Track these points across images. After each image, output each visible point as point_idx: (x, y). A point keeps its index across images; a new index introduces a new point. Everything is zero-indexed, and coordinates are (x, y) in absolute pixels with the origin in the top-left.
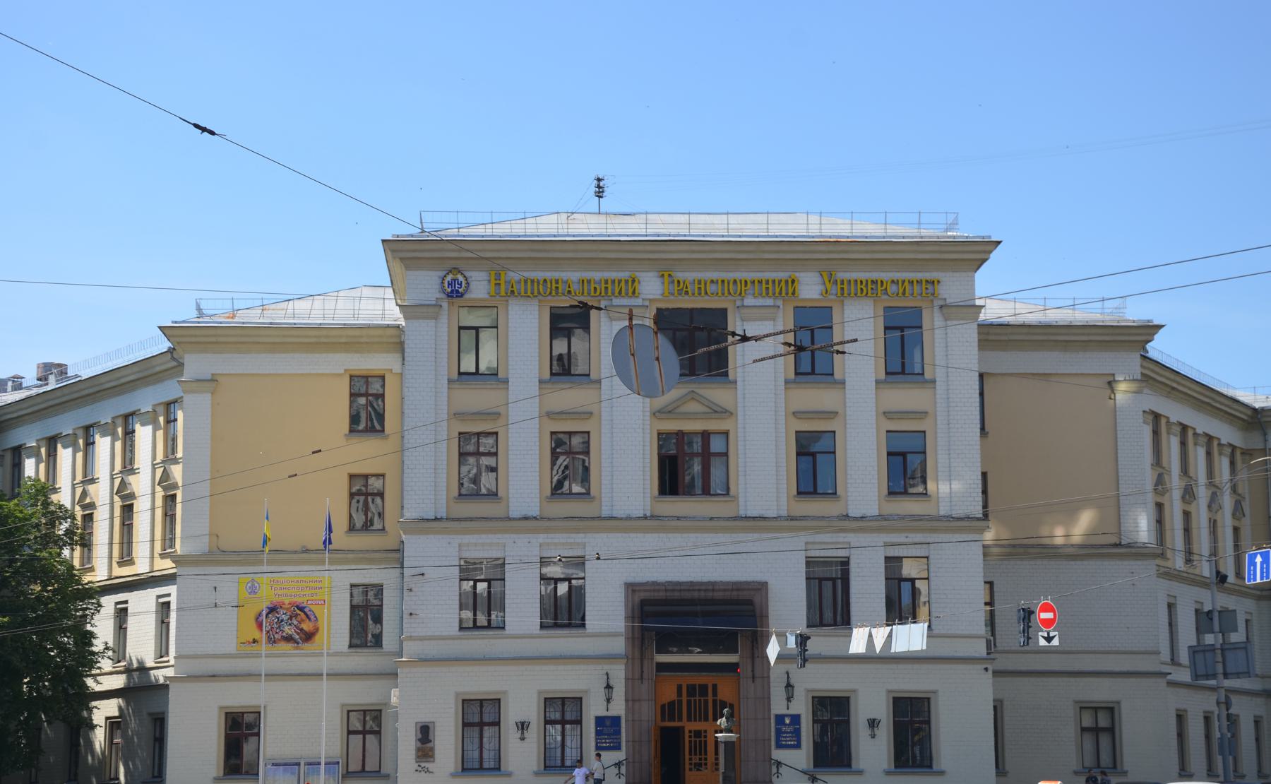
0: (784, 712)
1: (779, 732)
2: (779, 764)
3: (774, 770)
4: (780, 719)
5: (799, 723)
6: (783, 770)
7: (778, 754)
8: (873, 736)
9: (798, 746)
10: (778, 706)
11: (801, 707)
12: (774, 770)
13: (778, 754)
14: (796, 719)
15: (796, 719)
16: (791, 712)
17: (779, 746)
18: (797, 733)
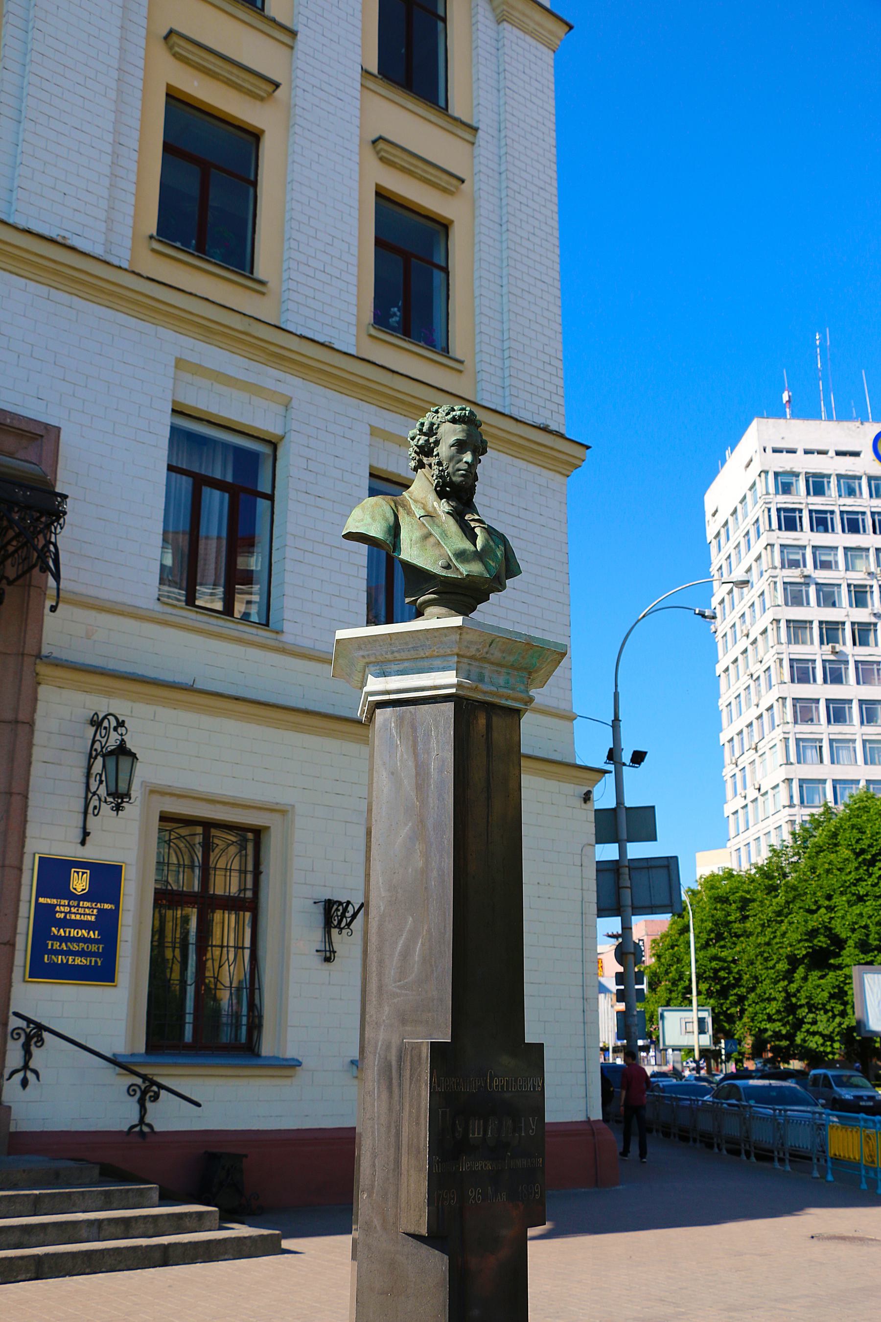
0: (69, 850)
1: (45, 918)
2: (35, 1033)
3: (14, 1056)
4: (54, 873)
5: (115, 899)
6: (48, 1055)
7: (35, 998)
8: (328, 956)
9: (103, 972)
10: (51, 834)
11: (125, 841)
12: (14, 1056)
13: (35, 998)
14: (107, 879)
15: (107, 879)
16: (92, 853)
17: (41, 970)
18: (108, 925)
